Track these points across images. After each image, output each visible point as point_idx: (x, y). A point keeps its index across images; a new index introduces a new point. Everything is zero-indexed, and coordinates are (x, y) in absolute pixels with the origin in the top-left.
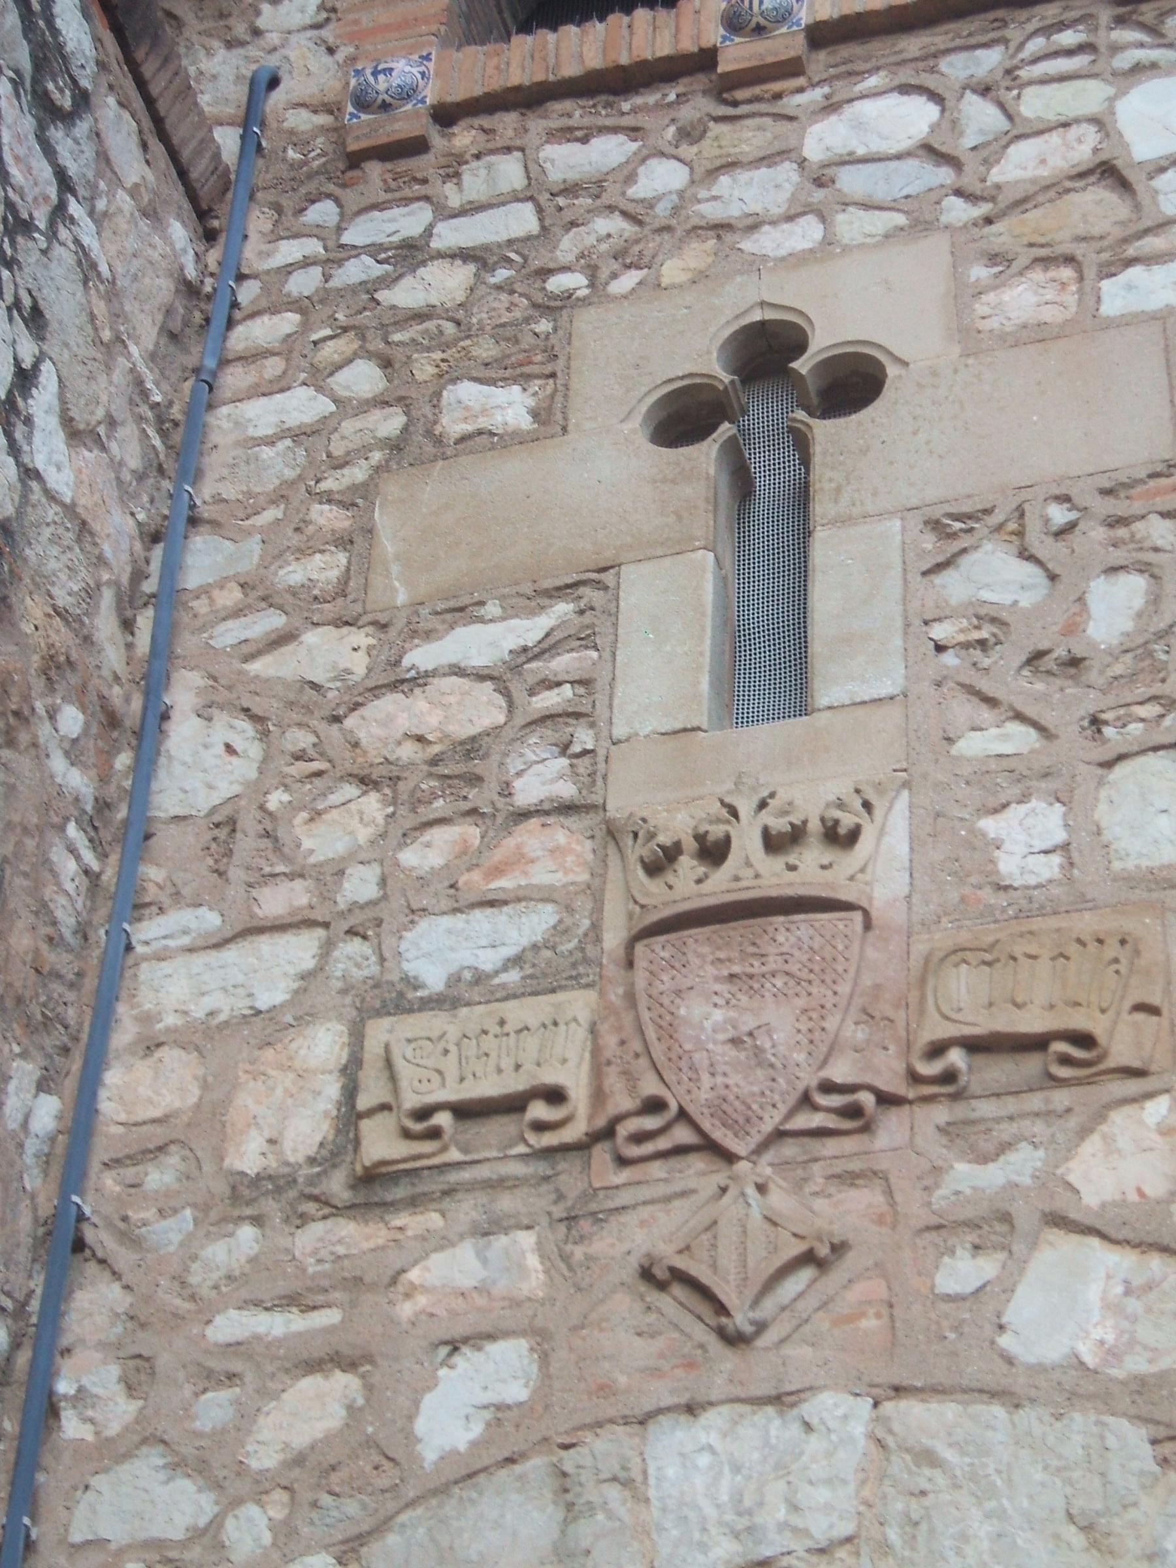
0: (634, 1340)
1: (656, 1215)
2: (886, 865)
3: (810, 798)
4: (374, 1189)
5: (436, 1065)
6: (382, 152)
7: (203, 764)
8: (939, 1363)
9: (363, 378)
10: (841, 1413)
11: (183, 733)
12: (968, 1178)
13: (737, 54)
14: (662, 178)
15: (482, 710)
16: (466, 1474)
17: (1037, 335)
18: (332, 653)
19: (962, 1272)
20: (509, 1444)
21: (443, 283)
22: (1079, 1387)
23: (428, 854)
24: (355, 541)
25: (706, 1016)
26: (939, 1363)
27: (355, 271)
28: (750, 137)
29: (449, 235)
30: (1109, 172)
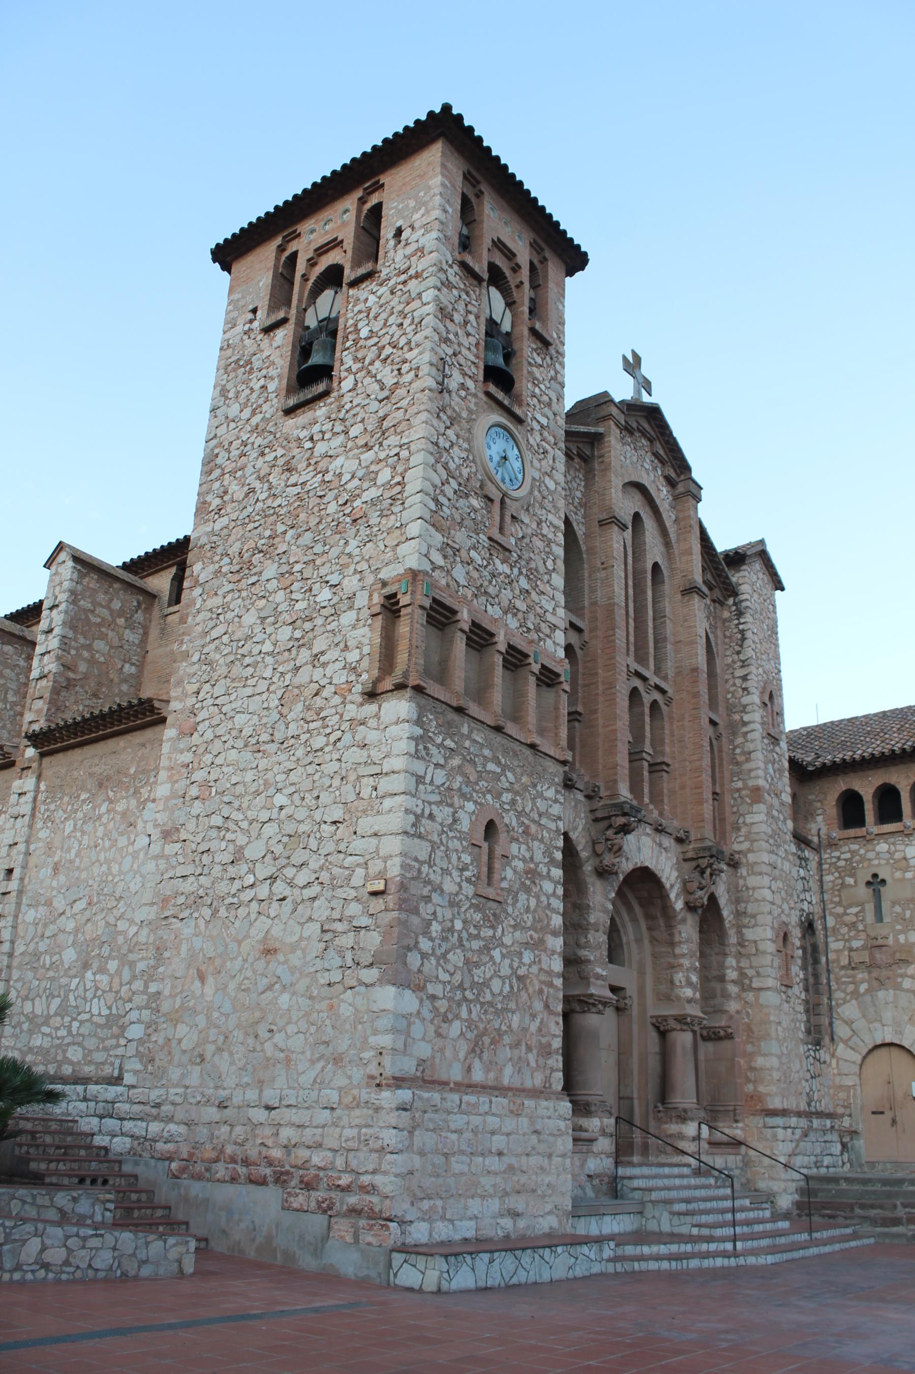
0: (875, 984)
1: (875, 974)
2: (891, 941)
3: (884, 932)
4: (853, 969)
5: (857, 958)
6: (833, 844)
7: (831, 922)
8: (898, 987)
9: (836, 875)
10: (891, 991)
11: (828, 918)
12: (900, 971)
13: (868, 837)
14: (862, 851)
15: (855, 919)
16: (864, 994)
17: (899, 880)
18: (840, 910)
19: (899, 980)
20: (867, 991)
21: (842, 863)
22: (908, 991)
23: (852, 934)
24: (840, 896)
25: (878, 956)
26: (898, 987)
27: (834, 860)
28: (870, 847)
29: (843, 856)
30: (905, 858)
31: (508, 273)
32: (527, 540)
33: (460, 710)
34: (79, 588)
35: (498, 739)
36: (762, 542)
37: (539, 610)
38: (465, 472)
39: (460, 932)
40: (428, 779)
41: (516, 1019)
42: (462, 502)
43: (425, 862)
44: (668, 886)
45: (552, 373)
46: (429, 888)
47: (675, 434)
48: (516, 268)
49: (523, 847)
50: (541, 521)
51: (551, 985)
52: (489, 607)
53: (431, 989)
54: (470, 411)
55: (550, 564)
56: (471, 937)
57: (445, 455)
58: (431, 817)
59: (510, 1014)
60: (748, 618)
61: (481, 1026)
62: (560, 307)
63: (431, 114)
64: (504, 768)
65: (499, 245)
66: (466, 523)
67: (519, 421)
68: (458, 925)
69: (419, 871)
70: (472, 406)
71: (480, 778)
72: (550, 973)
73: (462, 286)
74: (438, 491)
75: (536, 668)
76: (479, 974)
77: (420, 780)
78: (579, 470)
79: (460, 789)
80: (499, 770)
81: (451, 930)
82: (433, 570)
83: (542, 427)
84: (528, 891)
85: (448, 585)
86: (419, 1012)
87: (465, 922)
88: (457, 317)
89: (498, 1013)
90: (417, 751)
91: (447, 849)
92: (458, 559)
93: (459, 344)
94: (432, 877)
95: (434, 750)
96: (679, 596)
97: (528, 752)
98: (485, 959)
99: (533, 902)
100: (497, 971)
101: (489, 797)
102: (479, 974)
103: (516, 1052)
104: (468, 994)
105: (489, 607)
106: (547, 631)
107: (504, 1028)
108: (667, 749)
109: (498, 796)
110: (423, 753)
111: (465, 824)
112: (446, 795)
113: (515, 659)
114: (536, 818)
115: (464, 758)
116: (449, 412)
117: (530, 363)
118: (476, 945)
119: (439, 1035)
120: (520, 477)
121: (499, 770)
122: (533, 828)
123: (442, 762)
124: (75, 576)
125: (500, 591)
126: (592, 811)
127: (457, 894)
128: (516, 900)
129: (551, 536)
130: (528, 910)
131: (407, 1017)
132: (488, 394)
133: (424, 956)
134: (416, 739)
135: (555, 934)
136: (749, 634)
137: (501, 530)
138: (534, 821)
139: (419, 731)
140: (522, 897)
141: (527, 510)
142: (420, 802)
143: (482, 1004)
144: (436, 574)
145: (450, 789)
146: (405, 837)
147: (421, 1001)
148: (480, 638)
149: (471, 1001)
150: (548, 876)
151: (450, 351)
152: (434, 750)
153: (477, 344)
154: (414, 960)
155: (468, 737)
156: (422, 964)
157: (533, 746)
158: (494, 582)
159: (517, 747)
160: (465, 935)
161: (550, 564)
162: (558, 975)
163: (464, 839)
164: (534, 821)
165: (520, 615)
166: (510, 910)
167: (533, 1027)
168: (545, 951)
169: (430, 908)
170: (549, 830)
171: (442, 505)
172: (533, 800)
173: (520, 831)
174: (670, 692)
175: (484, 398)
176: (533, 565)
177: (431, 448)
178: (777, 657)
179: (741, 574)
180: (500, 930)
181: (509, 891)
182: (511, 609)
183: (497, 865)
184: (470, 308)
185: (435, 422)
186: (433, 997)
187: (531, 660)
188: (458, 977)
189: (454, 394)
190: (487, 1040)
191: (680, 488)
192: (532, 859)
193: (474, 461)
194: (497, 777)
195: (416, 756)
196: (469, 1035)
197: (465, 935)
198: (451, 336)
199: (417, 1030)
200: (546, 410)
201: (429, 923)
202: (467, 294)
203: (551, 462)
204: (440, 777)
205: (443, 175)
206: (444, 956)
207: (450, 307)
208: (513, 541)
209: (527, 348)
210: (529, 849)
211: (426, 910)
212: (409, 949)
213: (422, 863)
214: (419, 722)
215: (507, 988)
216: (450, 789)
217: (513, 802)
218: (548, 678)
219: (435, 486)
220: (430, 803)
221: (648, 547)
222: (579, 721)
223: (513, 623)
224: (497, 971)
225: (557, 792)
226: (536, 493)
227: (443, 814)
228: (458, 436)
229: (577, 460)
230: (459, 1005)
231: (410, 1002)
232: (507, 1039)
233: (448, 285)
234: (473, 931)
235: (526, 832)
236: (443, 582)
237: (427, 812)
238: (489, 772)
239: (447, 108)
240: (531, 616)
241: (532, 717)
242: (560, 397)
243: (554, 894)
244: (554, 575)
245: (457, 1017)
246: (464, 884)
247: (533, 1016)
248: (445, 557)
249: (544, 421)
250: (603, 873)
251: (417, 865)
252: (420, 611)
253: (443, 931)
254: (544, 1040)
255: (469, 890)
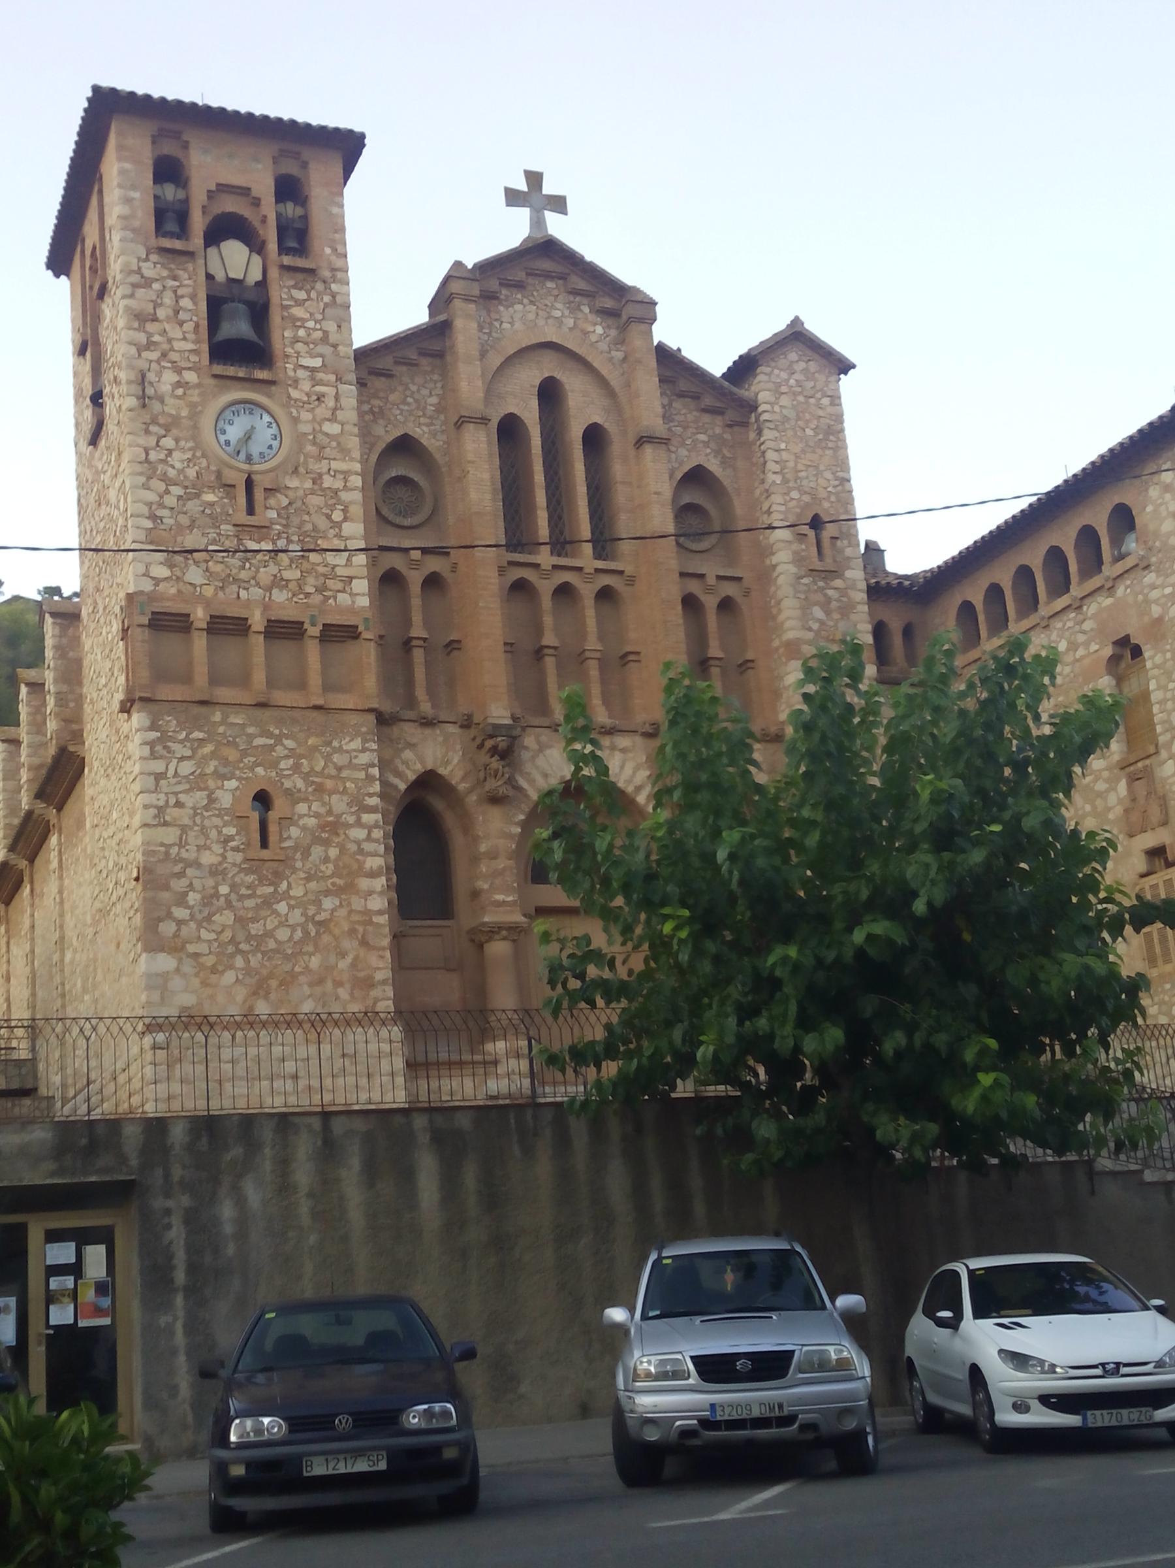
31: (245, 211)
32: (299, 504)
33: (203, 703)
34: (64, 641)
35: (267, 714)
36: (796, 321)
37: (321, 569)
38: (191, 473)
39: (227, 896)
40: (171, 773)
41: (315, 962)
42: (190, 504)
43: (174, 844)
44: (630, 789)
45: (327, 299)
46: (181, 865)
47: (588, 258)
48: (256, 203)
49: (315, 806)
50: (320, 475)
51: (370, 922)
52: (243, 594)
53: (191, 948)
54: (193, 406)
55: (337, 516)
56: (242, 898)
57: (160, 468)
58: (179, 804)
59: (306, 958)
60: (768, 434)
61: (265, 972)
62: (335, 210)
63: (89, 100)
64: (279, 739)
65: (224, 189)
66: (197, 523)
67: (273, 383)
68: (224, 890)
69: (167, 854)
70: (196, 399)
71: (244, 753)
72: (367, 912)
73: (165, 273)
74: (154, 507)
75: (315, 631)
76: (255, 929)
77: (159, 777)
78: (432, 372)
79: (216, 772)
80: (272, 741)
81: (216, 895)
82: (157, 585)
83: (313, 370)
84: (326, 843)
85: (179, 591)
86: (177, 970)
87: (234, 887)
88: (161, 313)
89: (287, 958)
90: (152, 752)
91: (203, 827)
92: (191, 562)
93: (170, 341)
94: (184, 855)
95: (174, 746)
96: (632, 452)
97: (315, 714)
98: (264, 913)
99: (333, 852)
100: (285, 921)
101: (260, 770)
102: (255, 929)
103: (318, 990)
104: (243, 946)
105: (243, 594)
106: (340, 586)
107: (297, 969)
108: (633, 635)
109: (274, 765)
110: (165, 753)
111: (226, 800)
112: (197, 782)
113: (283, 631)
114: (333, 772)
115: (219, 744)
116: (161, 420)
117: (287, 308)
118: (250, 903)
119: (205, 984)
120: (275, 444)
121: (272, 741)
122: (329, 784)
123: (189, 753)
124: (57, 631)
125: (257, 571)
126: (474, 739)
127: (220, 863)
128: (306, 853)
129: (339, 484)
130: (326, 860)
131: (165, 976)
132: (215, 376)
133: (180, 923)
134: (152, 744)
135: (372, 875)
136: (770, 455)
137: (251, 511)
138: (330, 777)
139: (155, 735)
140: (317, 851)
141: (295, 471)
142: (162, 796)
143: (264, 953)
144: (162, 587)
145: (203, 775)
146: (146, 829)
147: (180, 960)
148: (229, 627)
149: (248, 952)
150: (359, 823)
151: (154, 355)
152: (174, 746)
153: (197, 326)
154: (167, 929)
155: (223, 722)
156: (179, 930)
157: (317, 708)
158: (248, 565)
159: (297, 714)
160: (233, 897)
161: (337, 516)
162: (380, 913)
163: (226, 814)
164: (330, 777)
165: (293, 585)
166: (299, 864)
167: (343, 964)
168: (357, 892)
169: (184, 882)
170: (353, 780)
171: (161, 518)
172: (328, 758)
173: (310, 789)
174: (629, 570)
175: (212, 381)
176: (309, 527)
177: (139, 468)
178: (841, 464)
179: (759, 378)
180: (284, 885)
181: (295, 848)
182: (278, 582)
183: (273, 829)
184: (180, 292)
185: (142, 441)
186: (196, 955)
187: (306, 626)
188: (228, 935)
189: (168, 400)
190: (274, 983)
191: (624, 317)
192: (330, 812)
193: (204, 456)
194: (271, 748)
195: (153, 756)
196: (248, 980)
197: (233, 897)
198: (156, 338)
199: (176, 983)
200: (321, 349)
201: (186, 894)
202: (175, 278)
203: (331, 404)
204: (186, 768)
205: (120, 159)
206: (209, 919)
207: (151, 306)
208: (273, 514)
209: (281, 292)
210: (324, 804)
211: (179, 885)
212: (160, 920)
213: (171, 845)
214: (153, 727)
215: (299, 934)
216: (203, 775)
217: (296, 768)
218: (338, 634)
219: (149, 504)
220: (176, 794)
221: (572, 412)
222: (459, 649)
223: (279, 596)
224: (285, 921)
225: (364, 741)
226: (310, 448)
227: (200, 797)
228: (177, 440)
229: (425, 362)
230: (232, 956)
231: (165, 962)
232: (302, 979)
233: (147, 283)
234: (243, 891)
235: (320, 789)
236: (173, 591)
237: (172, 801)
238: (257, 747)
239: (96, 89)
240: (311, 580)
241: (315, 680)
242: (343, 323)
243: (369, 838)
244: (344, 525)
245: (231, 967)
246: (229, 854)
247: (343, 955)
248: (171, 566)
249: (317, 362)
250: (495, 800)
251: (162, 849)
252: (139, 630)
253: (203, 898)
254: (361, 975)
255: (239, 857)
